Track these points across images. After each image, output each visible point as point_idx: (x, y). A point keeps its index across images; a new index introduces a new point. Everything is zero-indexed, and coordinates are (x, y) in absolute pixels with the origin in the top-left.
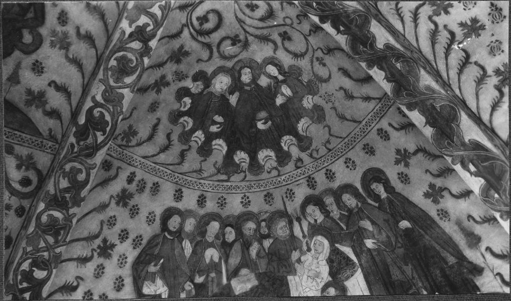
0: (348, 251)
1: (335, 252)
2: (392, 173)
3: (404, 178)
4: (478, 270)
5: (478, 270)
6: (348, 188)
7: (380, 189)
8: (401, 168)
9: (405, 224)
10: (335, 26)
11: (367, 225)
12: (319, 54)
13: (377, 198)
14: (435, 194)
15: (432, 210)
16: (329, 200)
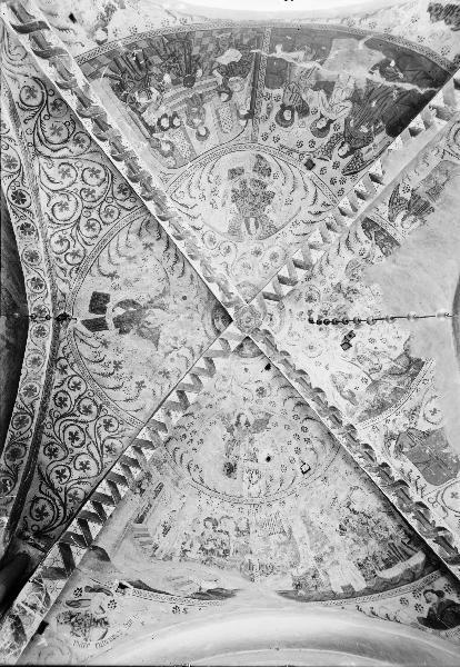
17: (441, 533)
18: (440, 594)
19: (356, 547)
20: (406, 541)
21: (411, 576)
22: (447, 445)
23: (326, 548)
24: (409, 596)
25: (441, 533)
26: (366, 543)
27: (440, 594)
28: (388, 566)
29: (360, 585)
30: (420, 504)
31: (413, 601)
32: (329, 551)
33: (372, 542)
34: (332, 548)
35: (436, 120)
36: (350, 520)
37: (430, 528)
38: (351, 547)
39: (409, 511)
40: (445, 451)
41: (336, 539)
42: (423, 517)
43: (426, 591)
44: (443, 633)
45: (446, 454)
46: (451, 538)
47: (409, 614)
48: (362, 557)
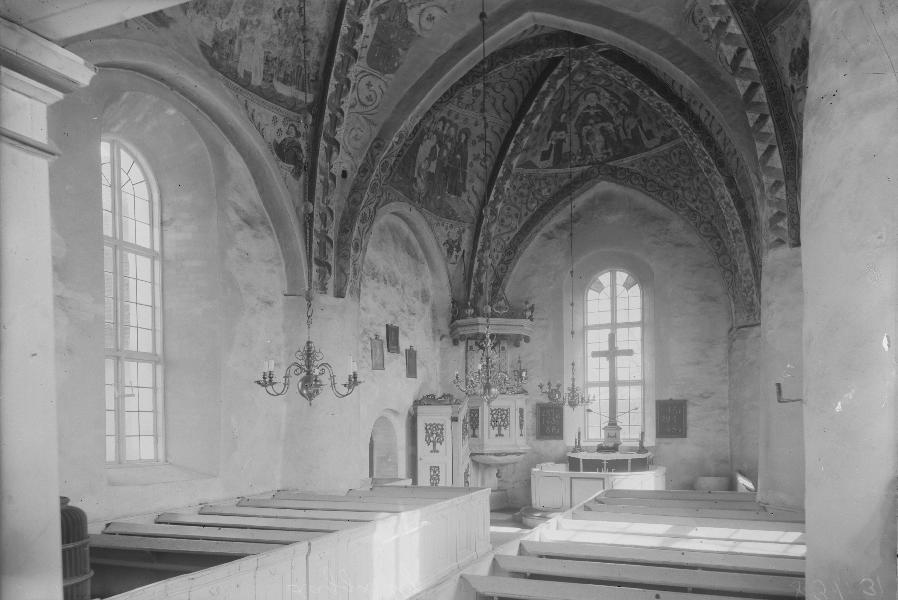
0: (438, 149)
1: (435, 147)
2: (473, 137)
3: (474, 143)
4: (465, 190)
5: (465, 190)
6: (456, 126)
7: (463, 137)
8: (477, 140)
9: (458, 156)
10: (535, 106)
11: (449, 145)
12: (507, 84)
13: (460, 140)
14: (476, 157)
15: (470, 160)
16: (448, 125)
17: (338, 114)
18: (298, 134)
19: (276, 40)
20: (311, 78)
21: (292, 105)
22: (405, 49)
23: (254, 19)
24: (281, 119)
25: (338, 114)
26: (285, 45)
27: (298, 134)
28: (284, 82)
29: (257, 80)
30: (348, 82)
31: (280, 125)
32: (255, 23)
33: (290, 50)
34: (259, 22)
35: (717, 19)
36: (291, 14)
37: (336, 104)
38: (273, 36)
39: (337, 77)
40: (400, 50)
41: (268, 18)
42: (341, 92)
43: (293, 125)
44: (281, 163)
45: (398, 54)
46: (341, 124)
47: (271, 133)
48: (274, 54)
